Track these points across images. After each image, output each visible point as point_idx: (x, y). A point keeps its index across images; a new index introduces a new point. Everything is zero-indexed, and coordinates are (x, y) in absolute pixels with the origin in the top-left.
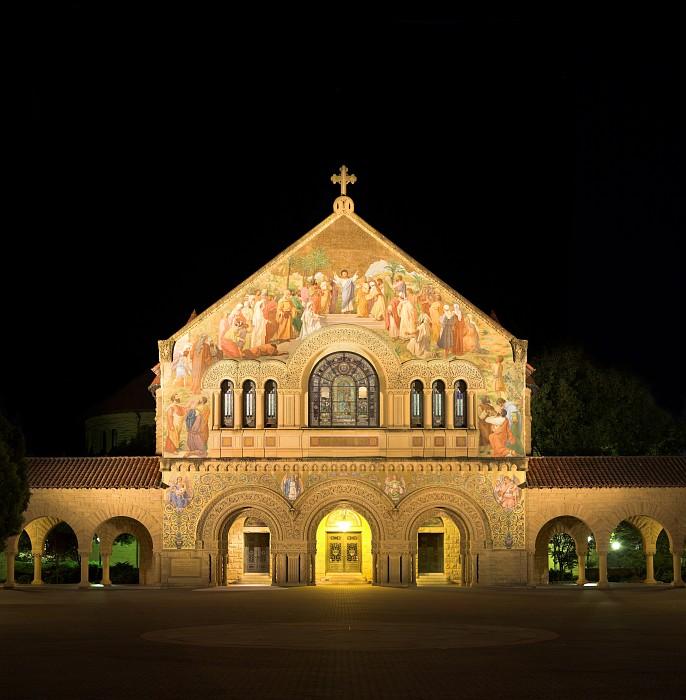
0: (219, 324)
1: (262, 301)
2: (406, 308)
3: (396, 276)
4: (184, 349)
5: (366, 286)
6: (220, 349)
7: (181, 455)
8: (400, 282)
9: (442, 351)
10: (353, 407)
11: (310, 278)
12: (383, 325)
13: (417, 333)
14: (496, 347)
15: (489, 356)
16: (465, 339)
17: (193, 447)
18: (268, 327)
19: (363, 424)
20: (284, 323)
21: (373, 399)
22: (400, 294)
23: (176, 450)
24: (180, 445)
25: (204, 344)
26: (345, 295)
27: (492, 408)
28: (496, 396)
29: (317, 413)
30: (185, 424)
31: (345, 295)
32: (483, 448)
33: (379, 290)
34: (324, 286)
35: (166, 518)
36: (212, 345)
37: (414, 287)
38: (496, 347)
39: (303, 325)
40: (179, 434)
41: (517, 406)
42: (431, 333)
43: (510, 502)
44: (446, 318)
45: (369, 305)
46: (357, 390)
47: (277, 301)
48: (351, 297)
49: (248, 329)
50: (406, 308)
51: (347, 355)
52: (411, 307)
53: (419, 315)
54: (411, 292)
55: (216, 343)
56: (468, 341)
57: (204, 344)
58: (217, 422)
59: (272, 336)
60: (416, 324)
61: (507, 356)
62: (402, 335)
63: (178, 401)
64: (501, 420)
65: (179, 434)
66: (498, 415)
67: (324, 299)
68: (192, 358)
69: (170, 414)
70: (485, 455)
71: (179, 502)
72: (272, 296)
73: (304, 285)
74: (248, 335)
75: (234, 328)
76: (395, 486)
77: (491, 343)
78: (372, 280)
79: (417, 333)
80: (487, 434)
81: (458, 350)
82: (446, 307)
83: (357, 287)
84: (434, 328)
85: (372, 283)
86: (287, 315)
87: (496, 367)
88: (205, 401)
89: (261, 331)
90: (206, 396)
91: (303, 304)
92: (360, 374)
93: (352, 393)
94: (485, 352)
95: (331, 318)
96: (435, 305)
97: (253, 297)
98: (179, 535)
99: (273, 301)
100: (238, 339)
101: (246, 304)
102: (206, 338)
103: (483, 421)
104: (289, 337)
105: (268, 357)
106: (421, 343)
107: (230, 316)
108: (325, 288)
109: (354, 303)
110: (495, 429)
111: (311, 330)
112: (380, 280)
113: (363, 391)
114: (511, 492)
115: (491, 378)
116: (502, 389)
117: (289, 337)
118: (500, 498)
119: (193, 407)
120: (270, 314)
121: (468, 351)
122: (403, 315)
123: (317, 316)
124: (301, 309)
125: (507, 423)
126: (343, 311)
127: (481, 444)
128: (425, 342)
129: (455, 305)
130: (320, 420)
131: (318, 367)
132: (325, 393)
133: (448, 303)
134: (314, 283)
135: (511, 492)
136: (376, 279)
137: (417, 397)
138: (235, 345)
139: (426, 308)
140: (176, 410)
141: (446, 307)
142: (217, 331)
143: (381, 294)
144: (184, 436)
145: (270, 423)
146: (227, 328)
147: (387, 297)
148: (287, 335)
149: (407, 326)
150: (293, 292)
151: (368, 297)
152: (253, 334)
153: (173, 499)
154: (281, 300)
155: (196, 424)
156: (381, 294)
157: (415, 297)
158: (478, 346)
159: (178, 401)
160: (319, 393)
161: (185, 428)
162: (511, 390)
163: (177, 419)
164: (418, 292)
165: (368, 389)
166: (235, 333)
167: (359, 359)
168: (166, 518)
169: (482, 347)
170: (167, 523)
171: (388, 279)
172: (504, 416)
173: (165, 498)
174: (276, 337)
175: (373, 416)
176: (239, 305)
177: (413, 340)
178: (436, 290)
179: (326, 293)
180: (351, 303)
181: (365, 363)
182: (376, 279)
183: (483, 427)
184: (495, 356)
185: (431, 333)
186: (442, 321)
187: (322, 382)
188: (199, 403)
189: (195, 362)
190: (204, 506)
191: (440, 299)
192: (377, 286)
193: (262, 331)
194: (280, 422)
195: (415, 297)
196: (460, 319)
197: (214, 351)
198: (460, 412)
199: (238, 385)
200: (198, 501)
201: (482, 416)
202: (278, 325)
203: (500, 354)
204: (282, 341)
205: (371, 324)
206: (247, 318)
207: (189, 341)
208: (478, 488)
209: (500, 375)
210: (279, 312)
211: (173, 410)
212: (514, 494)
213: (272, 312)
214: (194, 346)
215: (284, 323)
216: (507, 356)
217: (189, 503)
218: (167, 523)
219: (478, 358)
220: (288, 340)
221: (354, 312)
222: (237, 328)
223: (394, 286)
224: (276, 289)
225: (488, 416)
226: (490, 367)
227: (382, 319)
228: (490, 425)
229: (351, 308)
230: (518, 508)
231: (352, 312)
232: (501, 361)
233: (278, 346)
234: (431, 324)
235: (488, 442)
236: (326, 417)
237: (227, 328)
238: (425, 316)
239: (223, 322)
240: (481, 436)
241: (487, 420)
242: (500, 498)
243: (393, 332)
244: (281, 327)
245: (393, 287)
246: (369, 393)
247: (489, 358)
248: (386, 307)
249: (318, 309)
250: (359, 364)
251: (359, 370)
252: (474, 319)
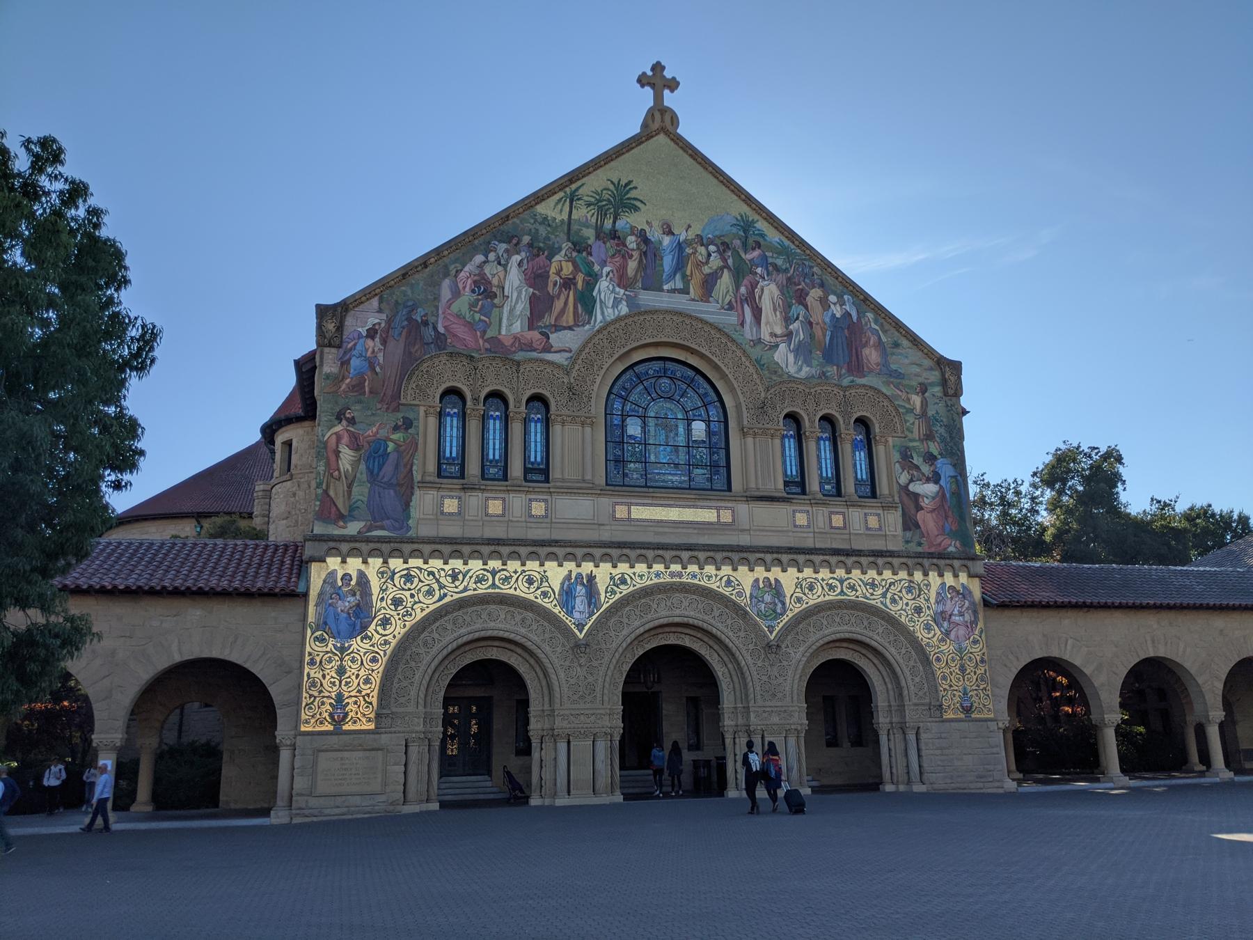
0: (439, 285)
1: (523, 254)
2: (769, 293)
3: (751, 241)
4: (369, 326)
5: (702, 250)
6: (441, 330)
7: (353, 528)
8: (756, 253)
9: (832, 370)
10: (682, 458)
11: (608, 224)
12: (733, 319)
13: (789, 335)
14: (916, 369)
15: (904, 382)
16: (866, 351)
17: (377, 516)
18: (533, 300)
19: (702, 486)
20: (563, 298)
21: (719, 443)
22: (759, 270)
23: (341, 517)
24: (351, 509)
25: (409, 319)
26: (668, 262)
27: (917, 468)
28: (922, 447)
29: (620, 462)
30: (363, 467)
31: (668, 262)
32: (909, 534)
33: (724, 260)
34: (631, 242)
35: (312, 662)
36: (426, 323)
37: (779, 262)
38: (916, 369)
39: (598, 305)
40: (350, 486)
41: (954, 466)
42: (812, 336)
43: (962, 631)
44: (833, 315)
45: (709, 283)
46: (689, 425)
47: (550, 258)
48: (680, 266)
49: (496, 301)
50: (769, 293)
51: (669, 365)
52: (776, 292)
53: (790, 307)
54: (777, 269)
55: (432, 319)
56: (871, 355)
57: (409, 319)
58: (432, 467)
59: (541, 317)
60: (787, 320)
61: (932, 384)
62: (765, 335)
63: (352, 421)
64: (931, 488)
65: (350, 486)
66: (928, 480)
67: (632, 265)
68: (384, 342)
69: (334, 446)
70: (913, 547)
71: (344, 626)
72: (539, 249)
73: (598, 237)
74: (496, 311)
75: (467, 296)
76: (768, 598)
77: (906, 361)
78: (712, 243)
79: (789, 335)
80: (913, 511)
81: (857, 367)
82: (833, 298)
83: (689, 251)
84: (818, 331)
85: (712, 248)
86: (568, 283)
87: (916, 400)
88: (408, 424)
89: (520, 307)
90: (411, 416)
91: (597, 268)
92: (692, 400)
93: (681, 430)
94: (899, 375)
95: (648, 299)
96: (815, 293)
97: (504, 246)
98: (340, 698)
99: (542, 257)
100: (477, 316)
101: (492, 256)
102: (413, 308)
103: (905, 488)
104: (571, 323)
105: (534, 355)
106: (797, 352)
107: (462, 274)
108: (634, 246)
109: (684, 277)
110: (925, 503)
111: (611, 314)
112: (726, 246)
113: (699, 428)
114: (961, 614)
115: (910, 418)
116: (929, 437)
117: (571, 323)
118: (946, 624)
119: (383, 433)
120: (536, 279)
121: (871, 371)
122: (766, 305)
123: (622, 291)
124: (592, 279)
125: (941, 494)
126: (665, 287)
127: (906, 528)
128: (802, 352)
129: (846, 297)
130: (625, 475)
131: (620, 382)
132: (634, 428)
133: (835, 293)
134: (614, 235)
135: (961, 614)
136: (718, 242)
137: (791, 445)
138: (471, 325)
139: (801, 298)
140: (345, 439)
141: (833, 298)
142: (437, 298)
143: (726, 266)
144: (360, 492)
145: (539, 473)
146: (456, 294)
147: (739, 273)
148: (569, 319)
149: (772, 323)
150: (580, 246)
151: (706, 270)
152: (506, 309)
153: (331, 621)
154: (557, 258)
155: (388, 469)
156: (726, 266)
157: (781, 278)
158: (886, 364)
159: (352, 421)
160: (623, 427)
161: (362, 474)
162: (943, 440)
163: (347, 456)
164: (786, 270)
165: (708, 426)
166: (472, 306)
167: (691, 373)
168: (312, 662)
169: (893, 367)
170: (315, 673)
171: (737, 243)
172: (937, 482)
173: (311, 617)
174: (549, 319)
175: (717, 473)
176: (479, 258)
177: (783, 347)
178: (815, 269)
179: (636, 254)
180: (678, 276)
181: (701, 380)
182: (718, 242)
183: (905, 499)
184: (914, 383)
185: (812, 336)
186: (827, 320)
187: (628, 408)
188: (396, 428)
189: (391, 344)
190: (398, 630)
191: (822, 285)
192: (721, 253)
193: (522, 307)
194: (555, 473)
195: (781, 278)
196: (855, 319)
197: (429, 333)
198: (863, 473)
199: (476, 400)
200: (385, 622)
201: (904, 478)
202: (551, 299)
203: (921, 380)
204: (557, 328)
205: (712, 313)
206: (495, 281)
207: (380, 311)
208: (907, 604)
209: (924, 413)
210: (553, 277)
211: (339, 438)
212: (967, 617)
213: (540, 276)
214: (389, 321)
215: (563, 298)
216: (932, 384)
217: (365, 627)
218: (315, 673)
219: (888, 384)
220: (570, 328)
221: (685, 291)
222: (475, 296)
223: (749, 256)
224: (548, 238)
225: (911, 481)
226: (909, 400)
227: (731, 307)
228: (916, 496)
229: (679, 285)
230: (976, 642)
231: (681, 291)
232: (923, 389)
233: (553, 337)
234: (811, 324)
235: (917, 526)
236: (636, 470)
237: (456, 294)
238: (802, 311)
239: (446, 283)
240: (904, 514)
241: (912, 487)
242: (946, 624)
243: (749, 332)
244: (559, 305)
245: (749, 256)
246: (709, 433)
247: (905, 386)
248: (738, 288)
249: (622, 280)
250: (690, 383)
251: (690, 393)
252: (876, 322)
